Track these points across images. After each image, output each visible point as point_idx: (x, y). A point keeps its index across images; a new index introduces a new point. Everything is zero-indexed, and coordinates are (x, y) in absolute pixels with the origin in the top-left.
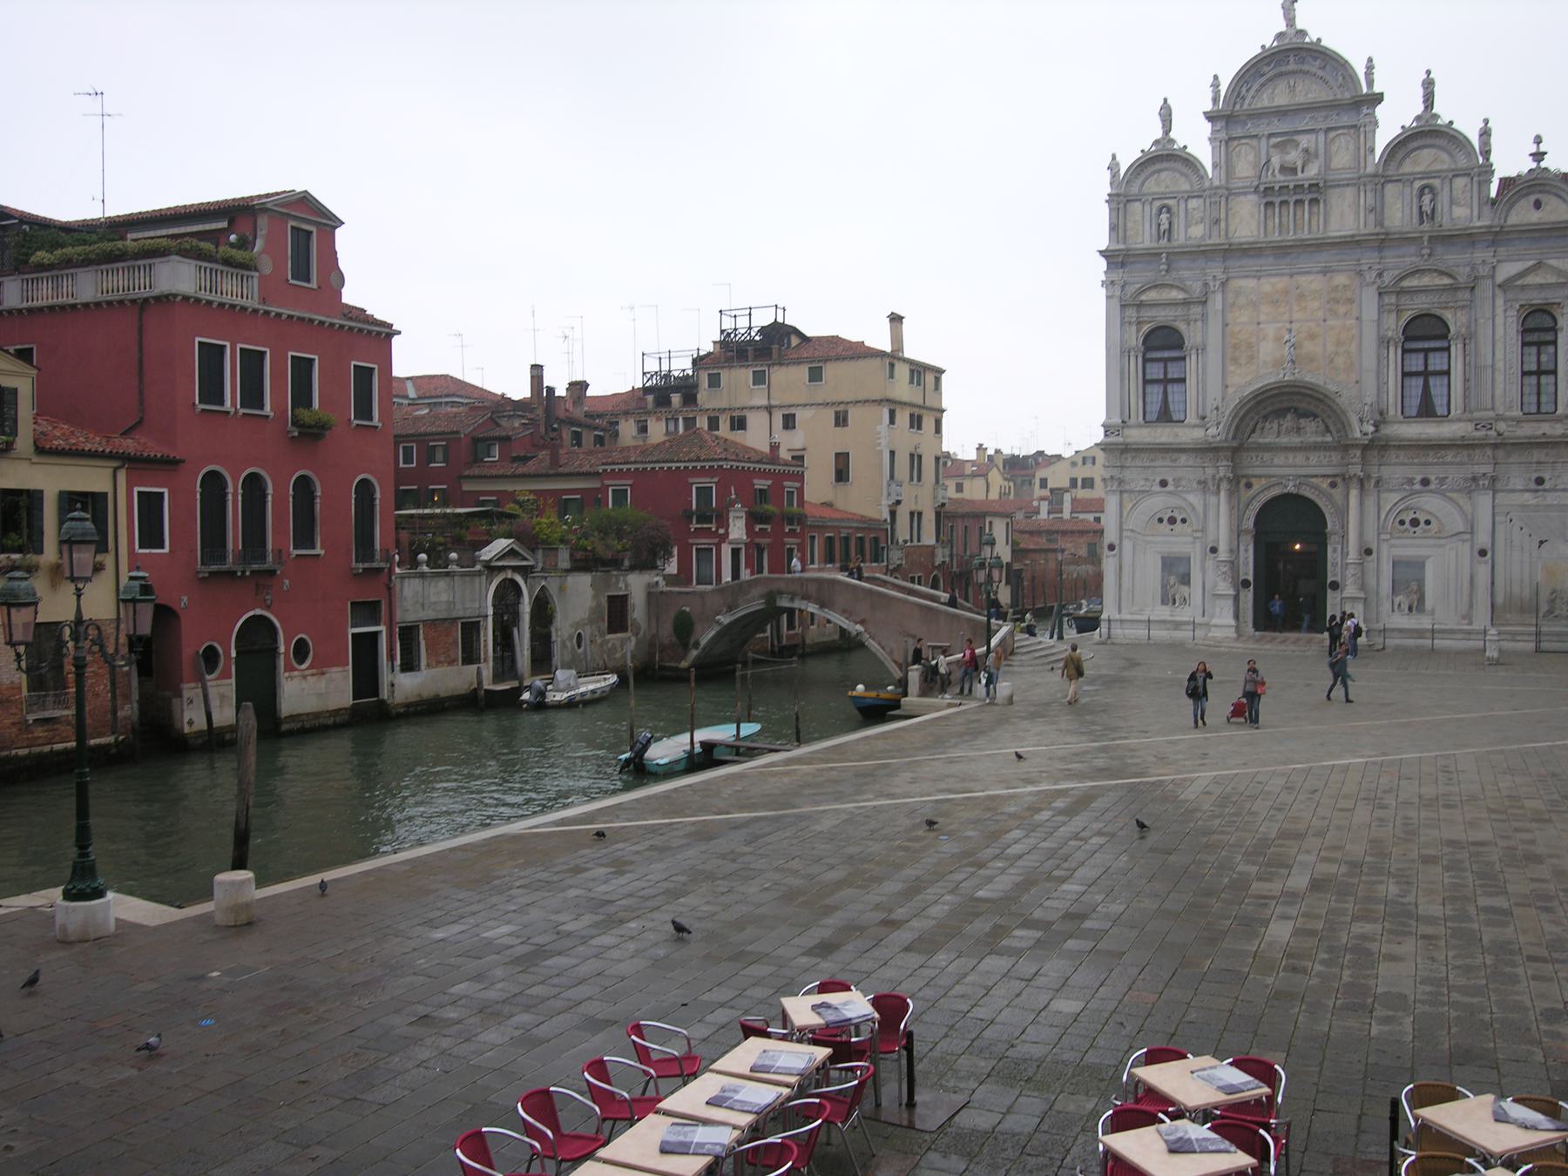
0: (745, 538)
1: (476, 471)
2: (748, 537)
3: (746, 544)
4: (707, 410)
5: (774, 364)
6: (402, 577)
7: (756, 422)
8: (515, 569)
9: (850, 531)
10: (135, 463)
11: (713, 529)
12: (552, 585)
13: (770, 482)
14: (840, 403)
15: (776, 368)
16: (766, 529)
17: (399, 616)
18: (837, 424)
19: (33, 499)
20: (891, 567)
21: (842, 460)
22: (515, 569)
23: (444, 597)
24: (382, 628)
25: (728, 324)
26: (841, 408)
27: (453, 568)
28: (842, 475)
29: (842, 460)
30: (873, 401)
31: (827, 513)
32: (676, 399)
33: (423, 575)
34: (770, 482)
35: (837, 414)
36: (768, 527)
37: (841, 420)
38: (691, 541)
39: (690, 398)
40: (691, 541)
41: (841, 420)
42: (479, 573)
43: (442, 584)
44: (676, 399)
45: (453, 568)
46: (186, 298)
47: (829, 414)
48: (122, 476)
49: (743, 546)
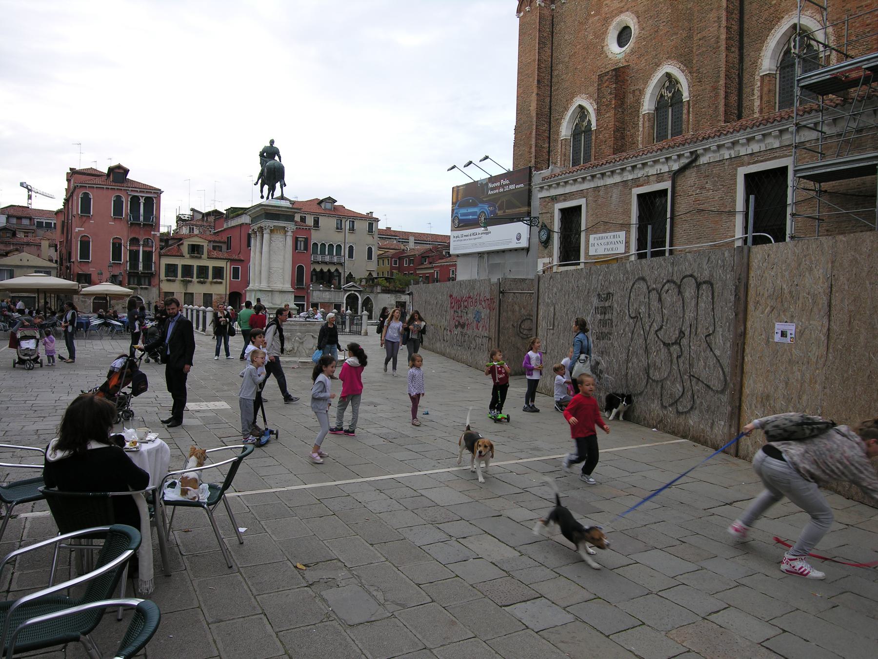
1: (419, 267)
6: (313, 291)
8: (355, 291)
10: (232, 261)
12: (372, 296)
17: (311, 300)
19: (207, 268)
22: (355, 291)
23: (328, 297)
24: (305, 303)
27: (321, 289)
33: (320, 290)
42: (341, 291)
43: (327, 293)
45: (332, 289)
46: (246, 224)
48: (229, 264)
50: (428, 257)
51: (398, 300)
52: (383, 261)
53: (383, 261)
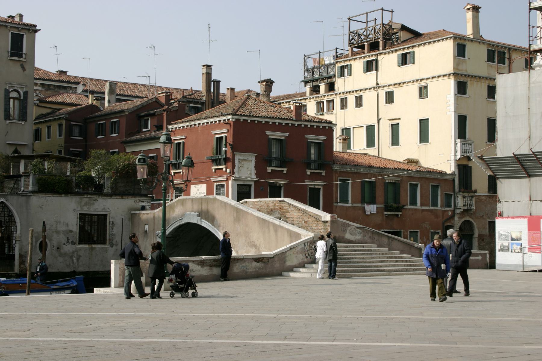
0: (254, 176)
2: (257, 175)
3: (256, 182)
4: (340, 93)
5: (381, 54)
7: (369, 98)
9: (399, 179)
11: (224, 170)
13: (287, 134)
14: (421, 80)
15: (382, 56)
16: (283, 171)
18: (421, 96)
20: (458, 211)
21: (424, 124)
25: (355, 26)
26: (423, 83)
28: (424, 137)
29: (424, 124)
30: (444, 76)
31: (413, 167)
32: (322, 88)
34: (287, 134)
35: (421, 88)
36: (285, 170)
37: (423, 92)
38: (213, 179)
39: (331, 87)
40: (213, 179)
41: (423, 92)
44: (322, 88)
47: (415, 89)
49: (253, 184)
50: (153, 115)
51: (86, 210)
52: (49, 128)
53: (49, 128)
